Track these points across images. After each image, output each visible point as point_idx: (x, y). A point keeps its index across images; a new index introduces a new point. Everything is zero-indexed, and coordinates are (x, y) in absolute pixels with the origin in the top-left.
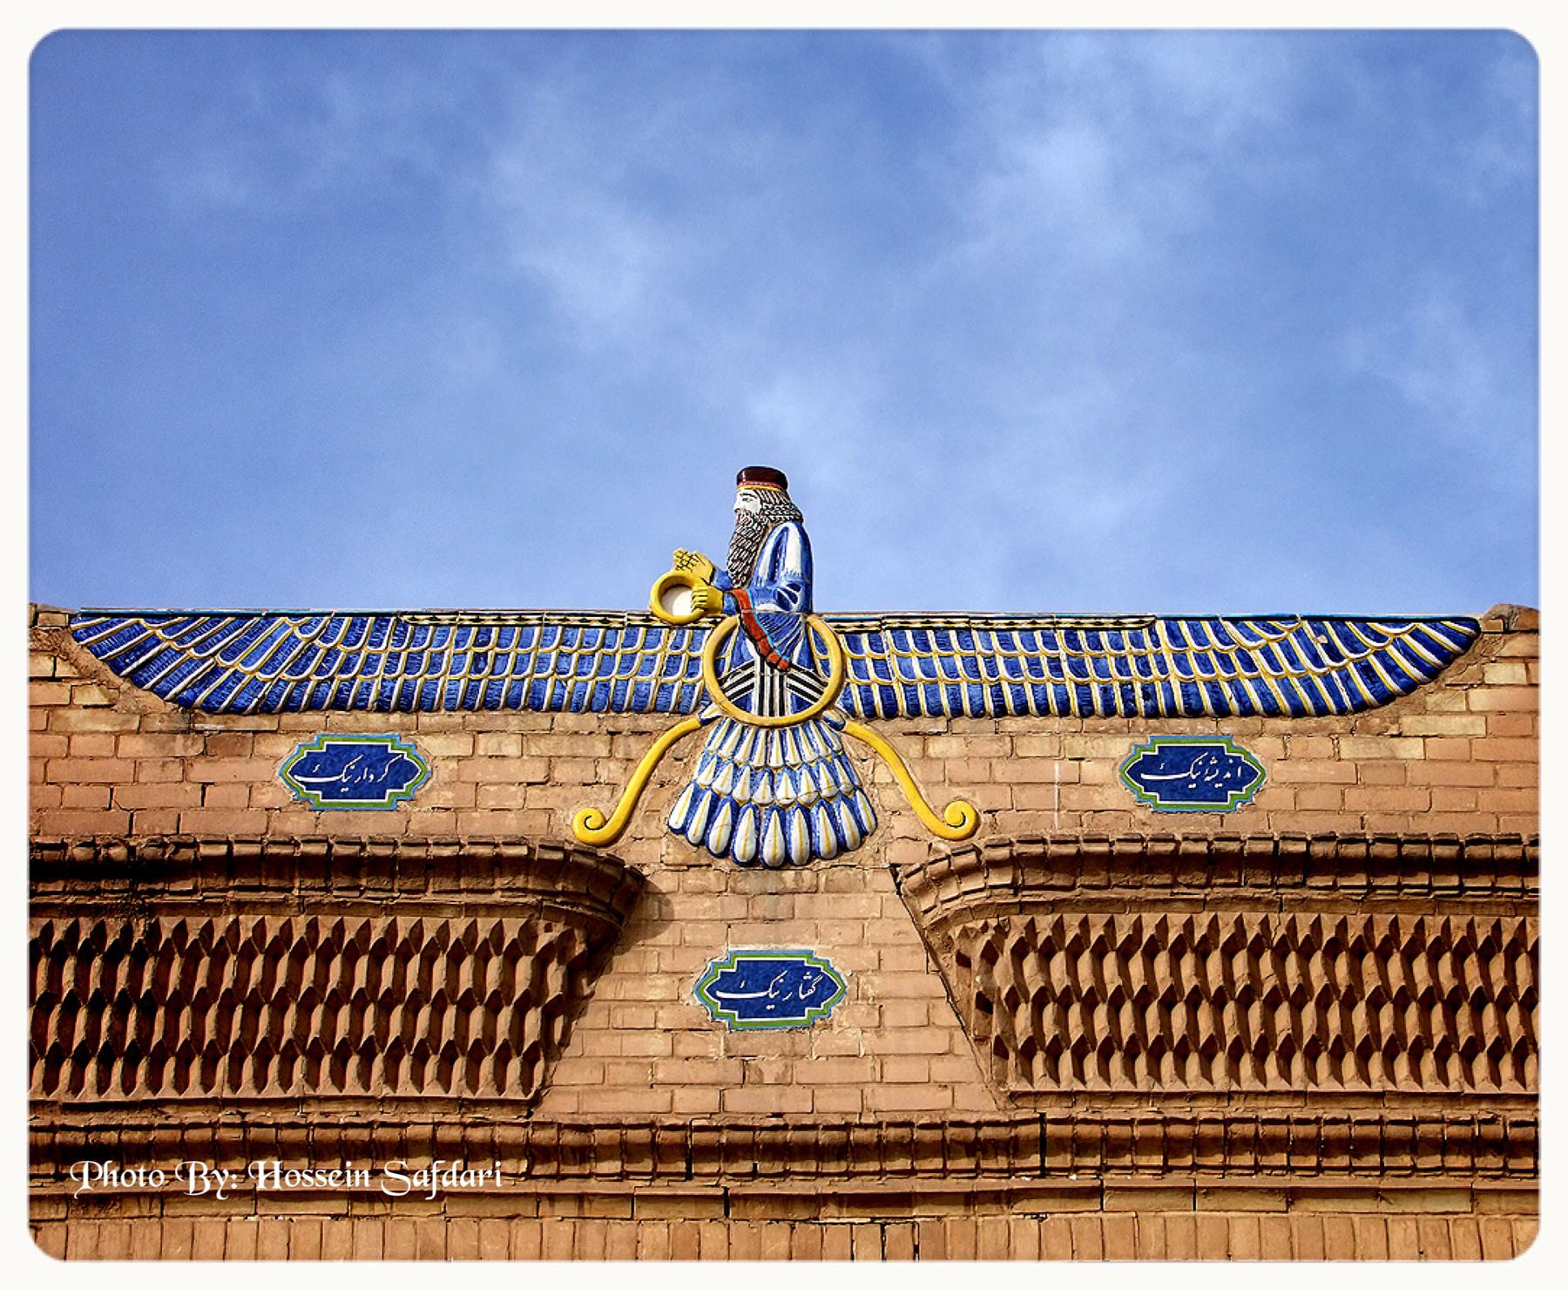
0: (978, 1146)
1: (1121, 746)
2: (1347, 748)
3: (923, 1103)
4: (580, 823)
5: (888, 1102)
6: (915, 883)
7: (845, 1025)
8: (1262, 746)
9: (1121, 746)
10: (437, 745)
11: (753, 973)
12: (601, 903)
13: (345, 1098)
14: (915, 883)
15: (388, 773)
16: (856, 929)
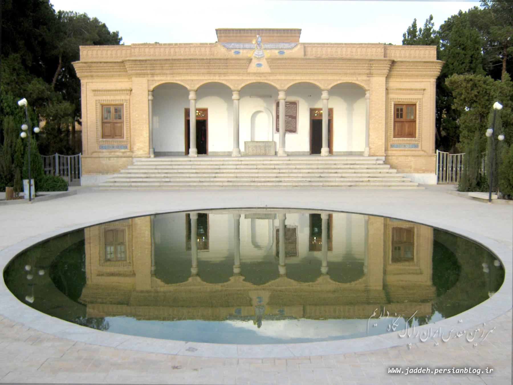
0: (269, 73)
1: (277, 51)
2: (290, 51)
3: (267, 71)
4: (249, 55)
5: (265, 71)
6: (267, 59)
7: (263, 67)
8: (285, 51)
9: (277, 51)
10: (241, 51)
11: (258, 64)
12: (250, 60)
13: (237, 71)
14: (267, 59)
15: (238, 53)
16: (264, 62)
